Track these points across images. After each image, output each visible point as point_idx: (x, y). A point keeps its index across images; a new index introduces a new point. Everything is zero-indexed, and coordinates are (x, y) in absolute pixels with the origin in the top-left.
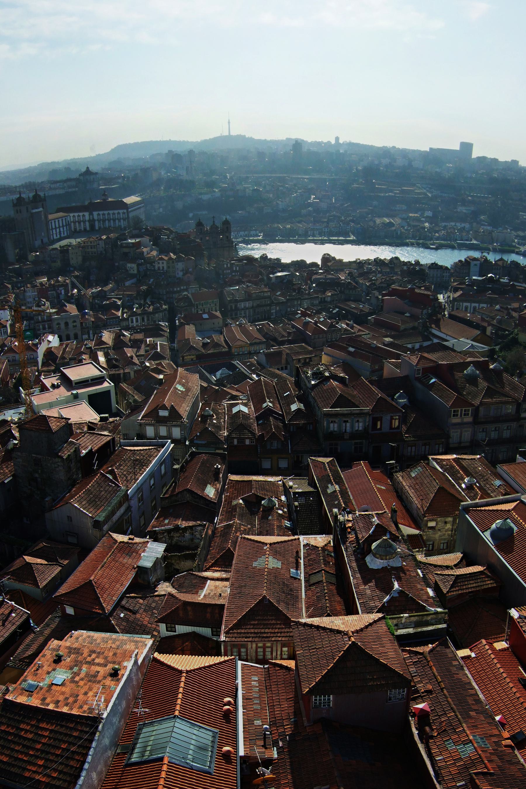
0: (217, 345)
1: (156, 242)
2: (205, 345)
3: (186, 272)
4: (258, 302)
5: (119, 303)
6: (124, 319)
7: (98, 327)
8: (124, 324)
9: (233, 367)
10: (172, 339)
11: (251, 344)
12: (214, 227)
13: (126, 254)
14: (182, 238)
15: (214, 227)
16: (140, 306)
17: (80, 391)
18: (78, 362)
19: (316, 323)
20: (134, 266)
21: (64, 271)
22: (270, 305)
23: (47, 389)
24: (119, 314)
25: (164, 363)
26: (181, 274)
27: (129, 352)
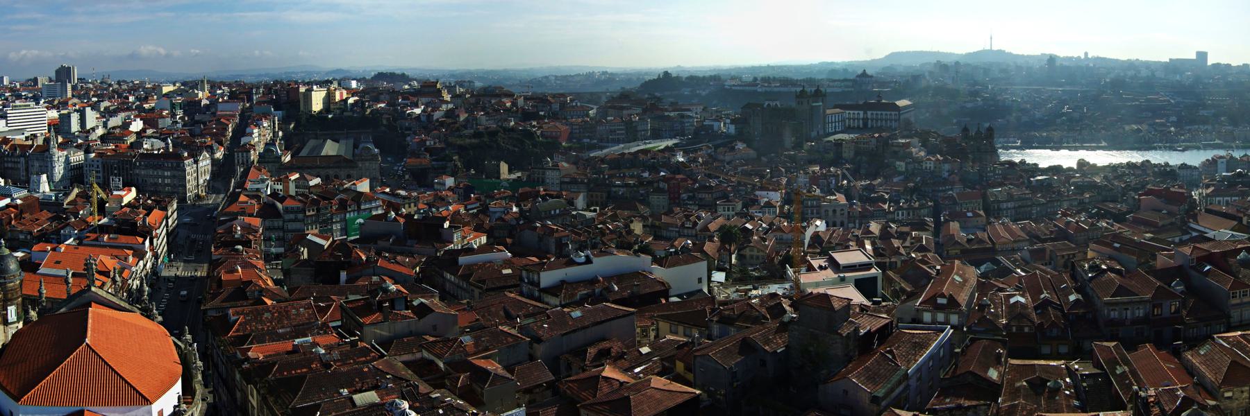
0: (981, 241)
1: (924, 144)
2: (969, 241)
3: (951, 172)
6: (890, 212)
7: (865, 218)
8: (890, 216)
9: (997, 262)
10: (936, 233)
11: (1015, 242)
13: (896, 153)
14: (949, 141)
16: (907, 201)
18: (846, 248)
19: (1077, 222)
20: (903, 164)
24: (886, 207)
25: (930, 255)
26: (946, 174)
27: (896, 243)
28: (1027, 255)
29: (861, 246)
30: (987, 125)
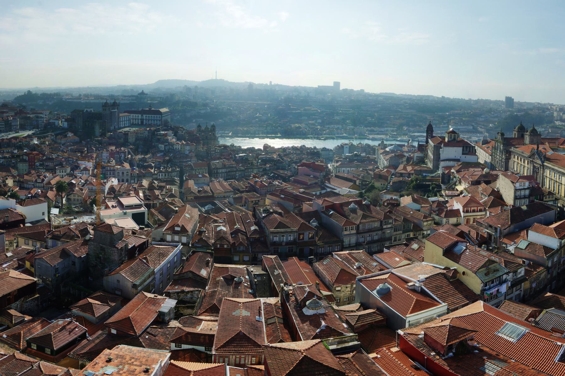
0: (206, 192)
1: (175, 135)
2: (199, 191)
3: (190, 151)
4: (229, 169)
5: (153, 165)
6: (155, 174)
7: (140, 177)
8: (155, 176)
9: (214, 204)
10: (181, 186)
11: (225, 192)
12: (207, 128)
13: (159, 139)
14: (190, 133)
15: (207, 128)
16: (164, 167)
17: (127, 211)
18: (129, 195)
20: (163, 146)
21: (124, 145)
22: (236, 171)
23: (109, 208)
24: (153, 171)
25: (176, 199)
26: (187, 152)
27: (157, 192)
28: (232, 200)
29: (137, 194)
30: (212, 123)
